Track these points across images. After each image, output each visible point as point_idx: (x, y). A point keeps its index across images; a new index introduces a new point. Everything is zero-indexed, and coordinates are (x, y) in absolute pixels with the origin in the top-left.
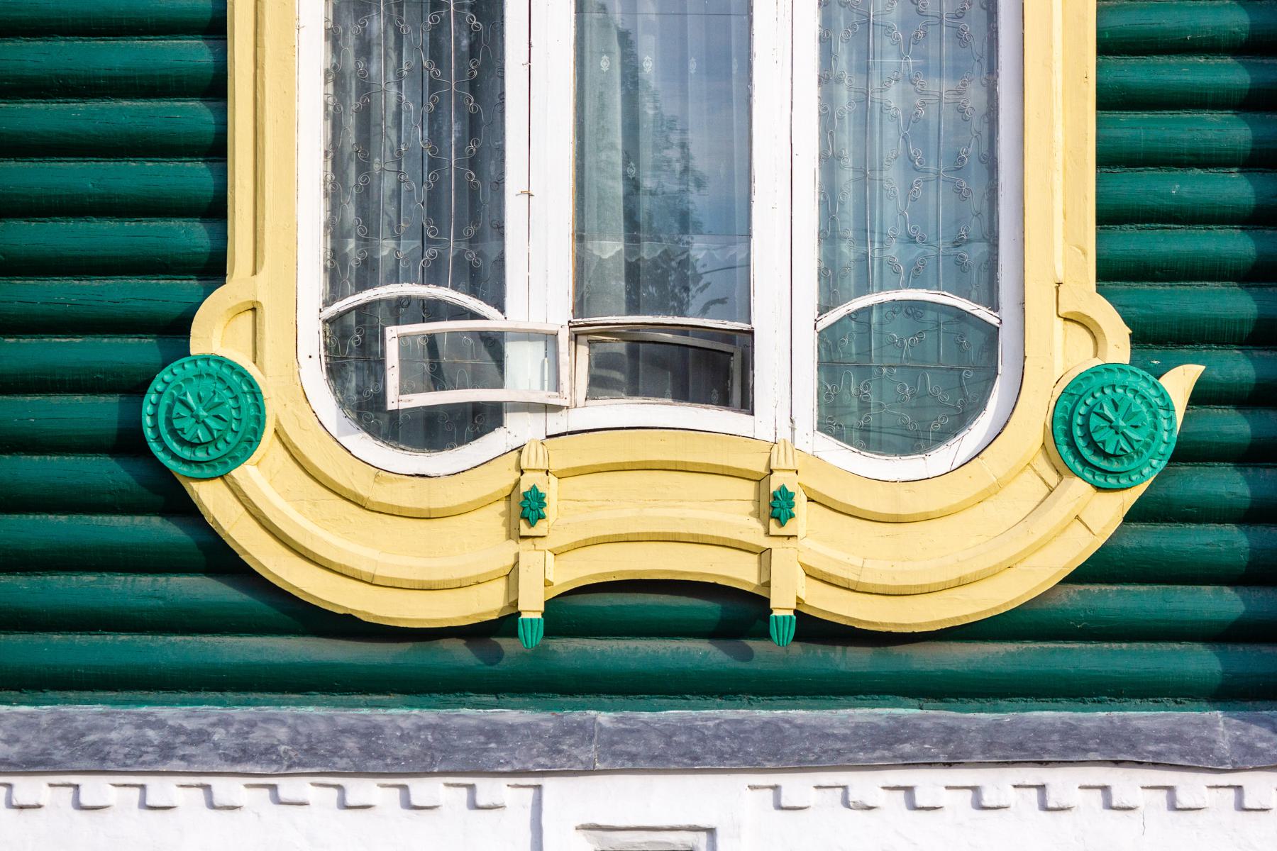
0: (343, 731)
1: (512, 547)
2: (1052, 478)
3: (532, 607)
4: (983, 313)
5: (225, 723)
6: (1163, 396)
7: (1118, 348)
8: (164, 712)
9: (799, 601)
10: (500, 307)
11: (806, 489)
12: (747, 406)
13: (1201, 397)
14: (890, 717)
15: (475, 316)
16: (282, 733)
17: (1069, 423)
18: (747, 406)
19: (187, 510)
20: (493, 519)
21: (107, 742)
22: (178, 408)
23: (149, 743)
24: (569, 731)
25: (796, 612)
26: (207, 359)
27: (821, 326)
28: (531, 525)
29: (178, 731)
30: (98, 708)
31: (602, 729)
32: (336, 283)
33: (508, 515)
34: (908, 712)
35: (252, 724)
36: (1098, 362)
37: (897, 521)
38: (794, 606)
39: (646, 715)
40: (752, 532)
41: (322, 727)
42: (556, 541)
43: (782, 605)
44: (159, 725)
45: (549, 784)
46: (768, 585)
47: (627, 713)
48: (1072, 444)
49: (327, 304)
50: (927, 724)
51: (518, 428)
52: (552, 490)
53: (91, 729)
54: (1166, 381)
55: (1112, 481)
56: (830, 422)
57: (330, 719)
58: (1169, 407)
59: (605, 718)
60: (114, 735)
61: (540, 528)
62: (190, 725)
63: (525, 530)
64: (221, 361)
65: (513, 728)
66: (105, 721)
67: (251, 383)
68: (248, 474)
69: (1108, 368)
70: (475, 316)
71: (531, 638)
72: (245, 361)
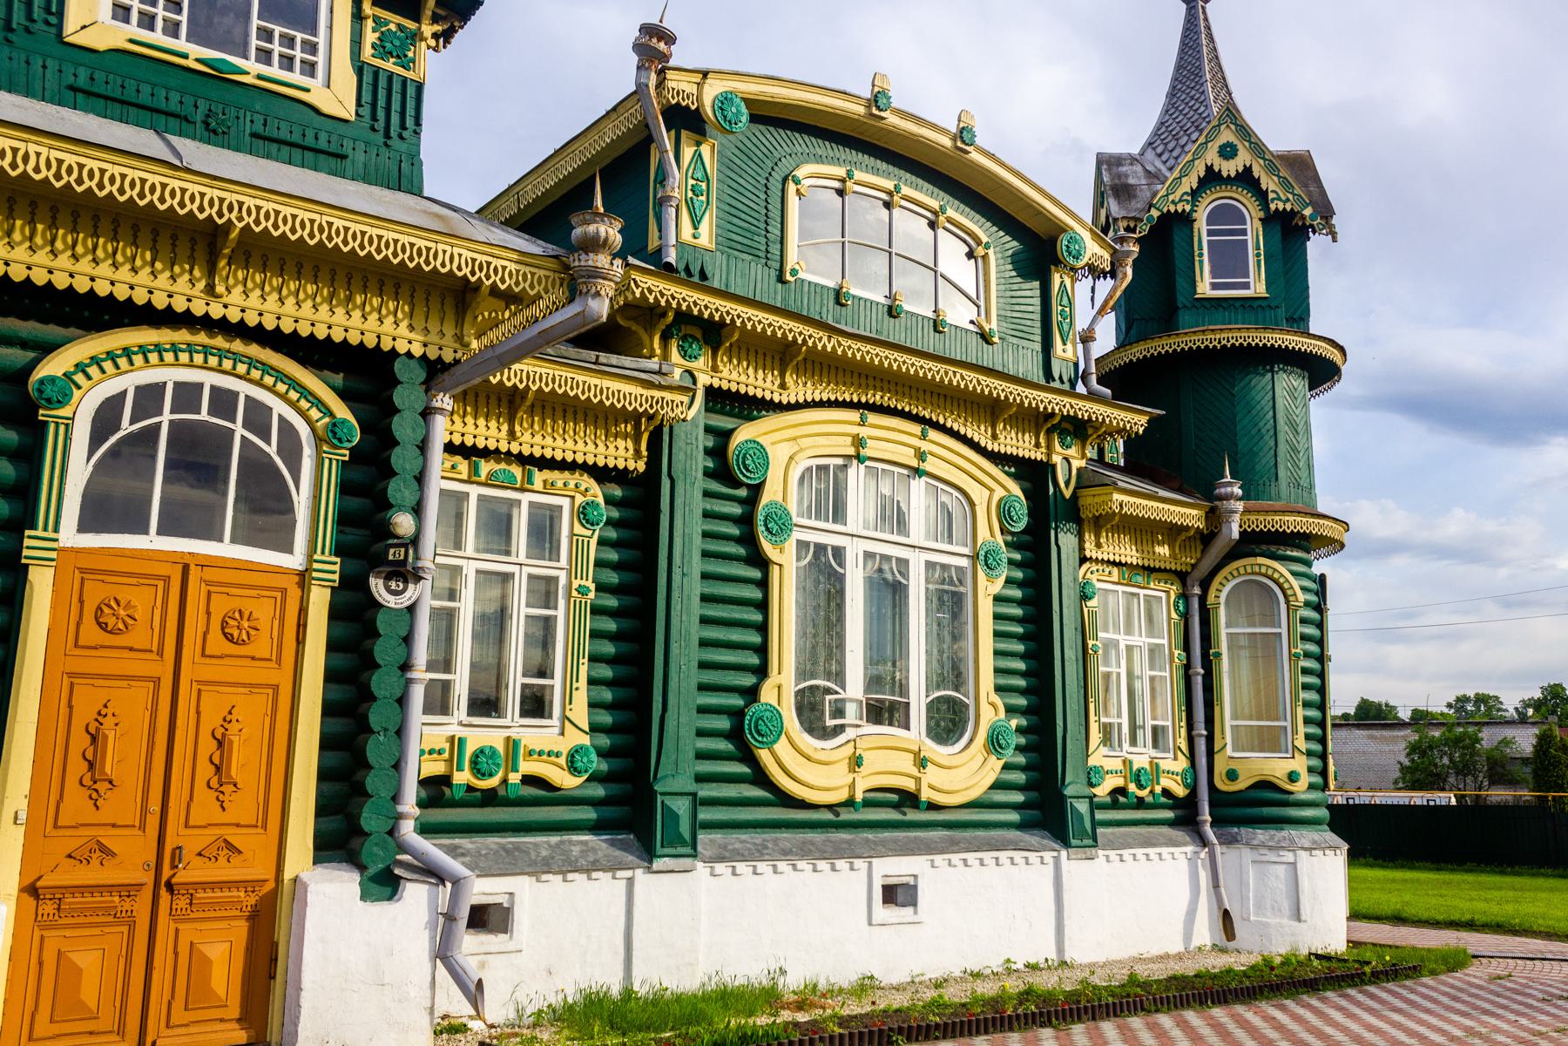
1: (851, 776)
2: (986, 755)
3: (859, 797)
8: (743, 837)
10: (844, 689)
15: (837, 693)
17: (992, 737)
19: (749, 758)
20: (844, 766)
22: (760, 722)
33: (850, 763)
36: (997, 718)
37: (949, 768)
40: (914, 771)
45: (875, 861)
48: (993, 744)
51: (850, 733)
52: (866, 755)
63: (857, 769)
67: (777, 711)
70: (837, 693)
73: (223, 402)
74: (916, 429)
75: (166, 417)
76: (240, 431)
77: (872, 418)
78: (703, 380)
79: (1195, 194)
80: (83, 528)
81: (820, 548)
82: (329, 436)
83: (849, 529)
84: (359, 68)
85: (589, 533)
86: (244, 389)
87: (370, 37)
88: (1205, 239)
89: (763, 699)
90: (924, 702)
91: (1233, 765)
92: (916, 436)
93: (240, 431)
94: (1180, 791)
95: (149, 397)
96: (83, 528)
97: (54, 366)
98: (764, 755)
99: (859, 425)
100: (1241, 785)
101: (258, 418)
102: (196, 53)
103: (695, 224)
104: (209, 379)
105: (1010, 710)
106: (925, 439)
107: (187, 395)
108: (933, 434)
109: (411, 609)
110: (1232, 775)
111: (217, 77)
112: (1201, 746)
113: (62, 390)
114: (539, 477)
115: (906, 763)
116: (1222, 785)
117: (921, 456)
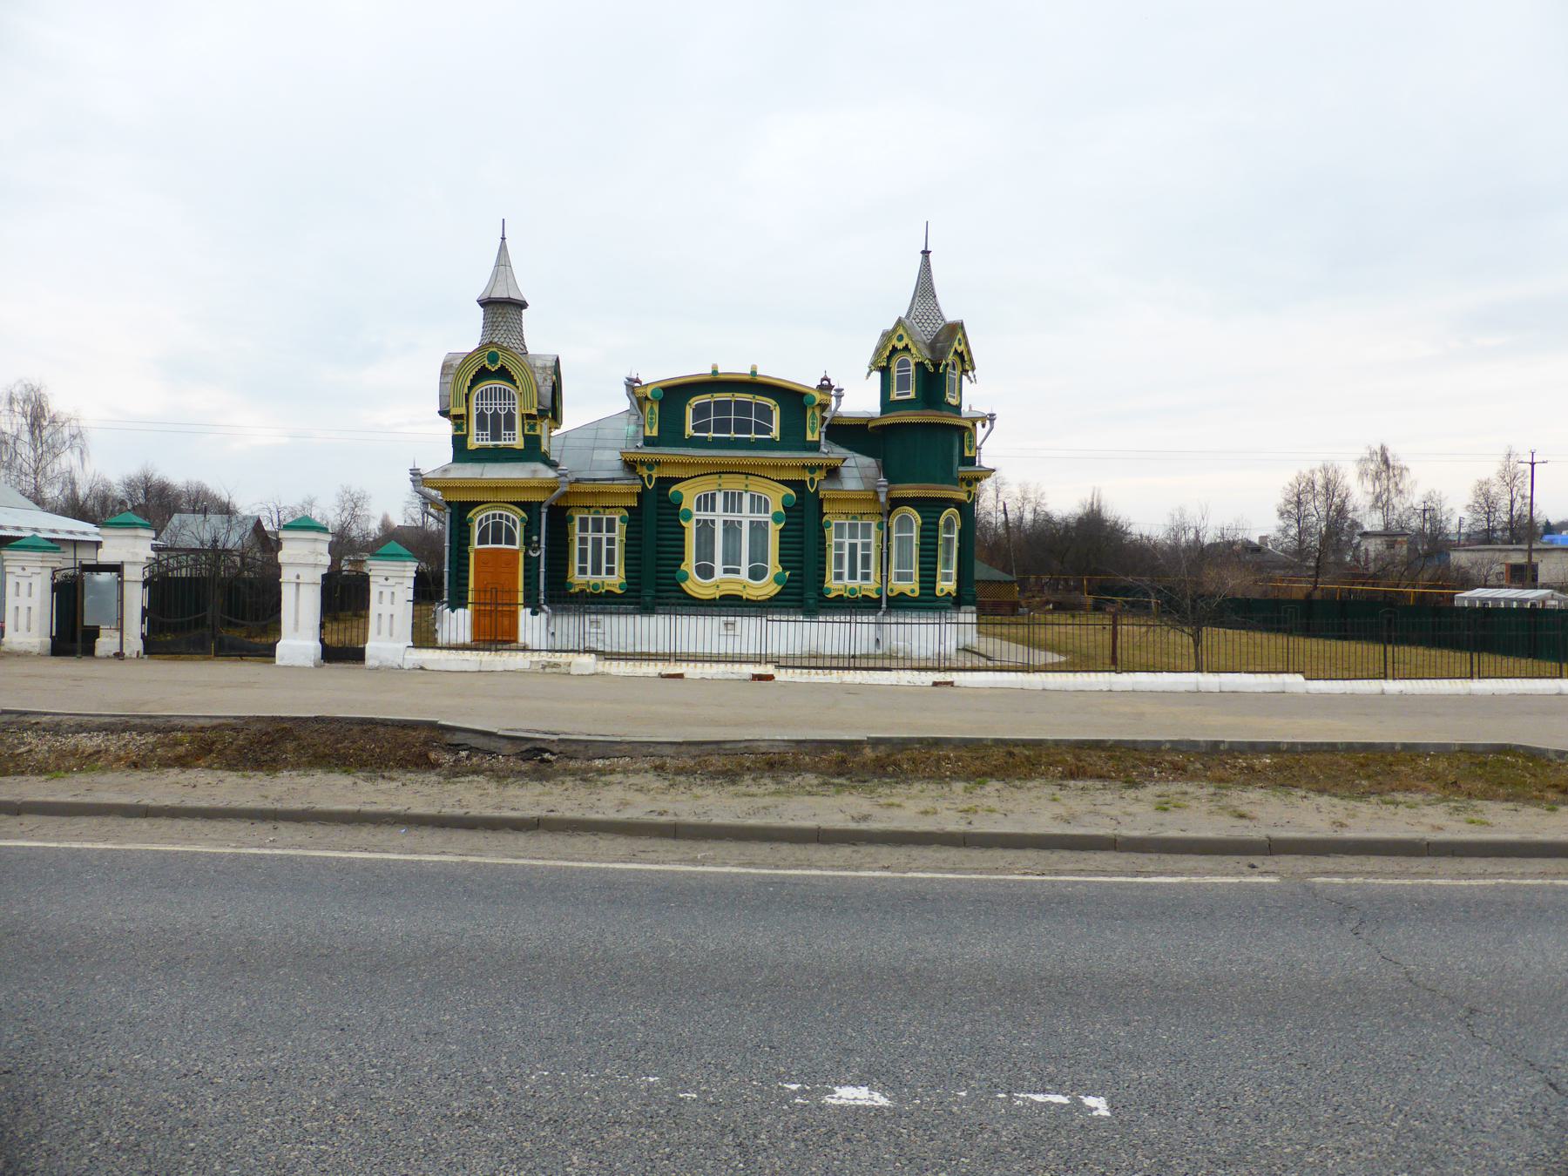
73: (501, 516)
74: (744, 476)
75: (491, 521)
76: (504, 522)
78: (655, 476)
79: (889, 358)
80: (479, 544)
82: (522, 520)
84: (524, 435)
86: (505, 513)
87: (526, 427)
88: (896, 374)
91: (893, 587)
93: (504, 522)
94: (875, 596)
95: (487, 518)
96: (479, 544)
97: (470, 515)
98: (683, 585)
100: (895, 594)
101: (507, 518)
102: (491, 443)
103: (651, 429)
104: (498, 512)
105: (785, 569)
107: (494, 516)
108: (750, 477)
109: (539, 556)
110: (892, 591)
111: (496, 448)
112: (884, 578)
113: (471, 520)
114: (607, 511)
115: (741, 588)
116: (889, 594)
117: (747, 486)
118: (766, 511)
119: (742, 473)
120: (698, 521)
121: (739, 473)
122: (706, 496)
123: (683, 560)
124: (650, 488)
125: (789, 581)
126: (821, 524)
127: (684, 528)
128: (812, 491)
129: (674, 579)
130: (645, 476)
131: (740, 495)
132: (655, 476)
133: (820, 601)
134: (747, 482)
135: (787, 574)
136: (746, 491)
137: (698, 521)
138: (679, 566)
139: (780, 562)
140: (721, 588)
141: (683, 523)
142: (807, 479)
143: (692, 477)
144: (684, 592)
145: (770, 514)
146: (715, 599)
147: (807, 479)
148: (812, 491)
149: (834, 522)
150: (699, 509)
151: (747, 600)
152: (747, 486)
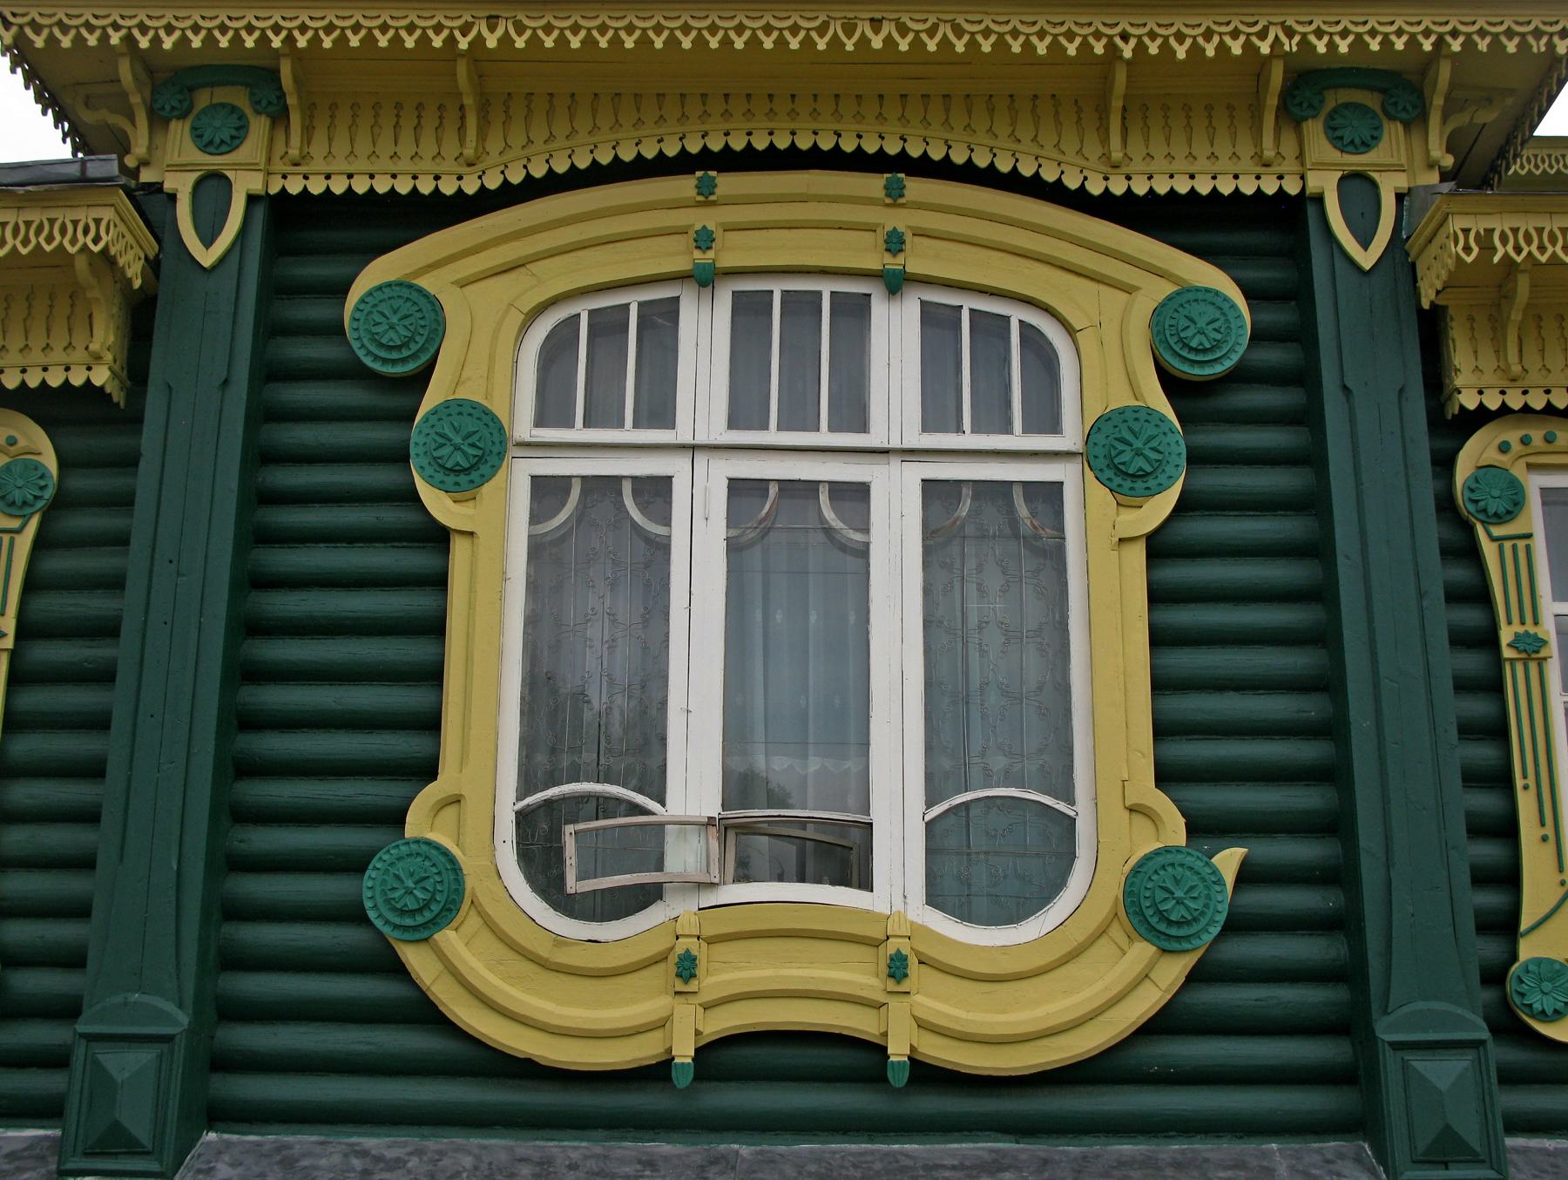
0: (520, 1160)
3: (684, 1052)
4: (1061, 806)
5: (419, 1152)
6: (1215, 872)
7: (1175, 831)
9: (913, 1048)
10: (663, 803)
11: (917, 953)
12: (866, 884)
13: (1248, 876)
14: (991, 1151)
16: (468, 1161)
18: (866, 884)
19: (398, 970)
21: (316, 1168)
23: (353, 1170)
24: (715, 1161)
25: (909, 1058)
26: (417, 841)
27: (928, 818)
28: (686, 982)
29: (379, 1159)
30: (314, 1138)
31: (744, 1160)
32: (527, 784)
34: (1006, 1145)
35: (442, 1153)
38: (909, 1053)
39: (782, 1149)
41: (503, 1157)
42: (706, 997)
43: (898, 1051)
44: (364, 1154)
46: (885, 1034)
47: (765, 1147)
49: (519, 799)
50: (1023, 1156)
53: (304, 1155)
54: (1216, 860)
55: (1176, 946)
56: (934, 898)
57: (511, 1149)
58: (1220, 882)
59: (745, 1150)
60: (323, 1162)
61: (693, 986)
62: (391, 1154)
63: (680, 987)
64: (429, 843)
65: (666, 1158)
66: (318, 1149)
67: (452, 860)
68: (448, 938)
69: (1167, 850)
71: (682, 1080)
72: (448, 843)
77: (728, 183)
78: (245, 184)
81: (606, 486)
83: (682, 434)
85: (15, 524)
89: (410, 831)
90: (916, 814)
92: (869, 201)
98: (415, 958)
99: (699, 205)
106: (894, 205)
108: (917, 188)
115: (860, 975)
117: (895, 243)
118: (1045, 417)
119: (859, 162)
120: (547, 491)
121: (835, 160)
122: (608, 326)
123: (428, 771)
124: (207, 257)
125: (1237, 925)
126: (1446, 504)
127: (439, 537)
128: (1367, 259)
129: (356, 916)
130: (181, 185)
131: (853, 312)
132: (245, 184)
133: (1510, 1078)
134: (898, 220)
135: (1229, 860)
136: (895, 283)
137: (547, 491)
138: (396, 818)
139: (1165, 777)
140: (715, 978)
141: (439, 505)
142: (1325, 183)
143: (509, 196)
144: (427, 1014)
145: (1070, 437)
146: (659, 1072)
147: (1325, 183)
148: (1367, 259)
149: (1534, 484)
150: (551, 410)
151: (925, 1074)
152: (895, 243)
